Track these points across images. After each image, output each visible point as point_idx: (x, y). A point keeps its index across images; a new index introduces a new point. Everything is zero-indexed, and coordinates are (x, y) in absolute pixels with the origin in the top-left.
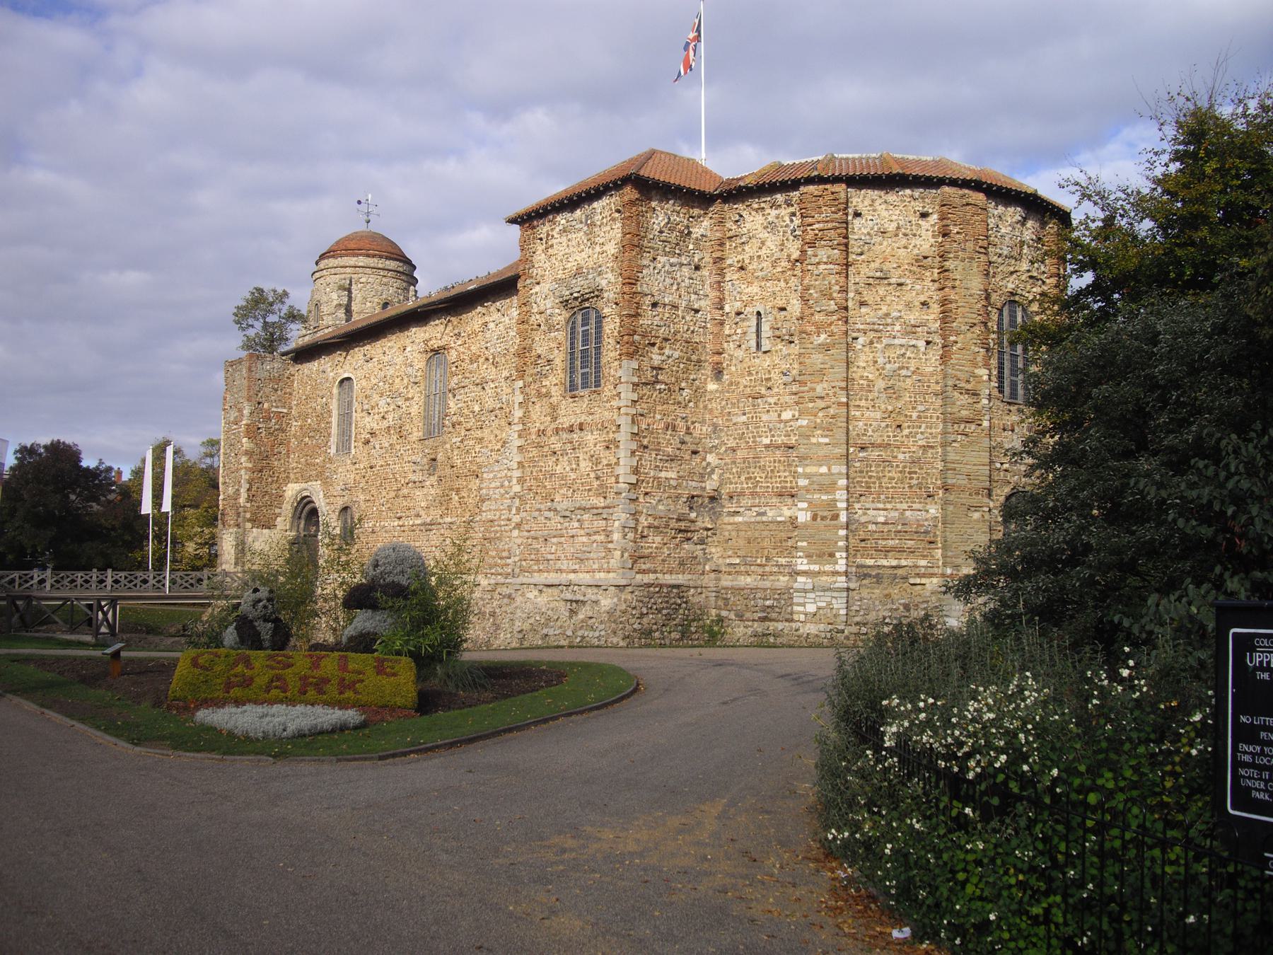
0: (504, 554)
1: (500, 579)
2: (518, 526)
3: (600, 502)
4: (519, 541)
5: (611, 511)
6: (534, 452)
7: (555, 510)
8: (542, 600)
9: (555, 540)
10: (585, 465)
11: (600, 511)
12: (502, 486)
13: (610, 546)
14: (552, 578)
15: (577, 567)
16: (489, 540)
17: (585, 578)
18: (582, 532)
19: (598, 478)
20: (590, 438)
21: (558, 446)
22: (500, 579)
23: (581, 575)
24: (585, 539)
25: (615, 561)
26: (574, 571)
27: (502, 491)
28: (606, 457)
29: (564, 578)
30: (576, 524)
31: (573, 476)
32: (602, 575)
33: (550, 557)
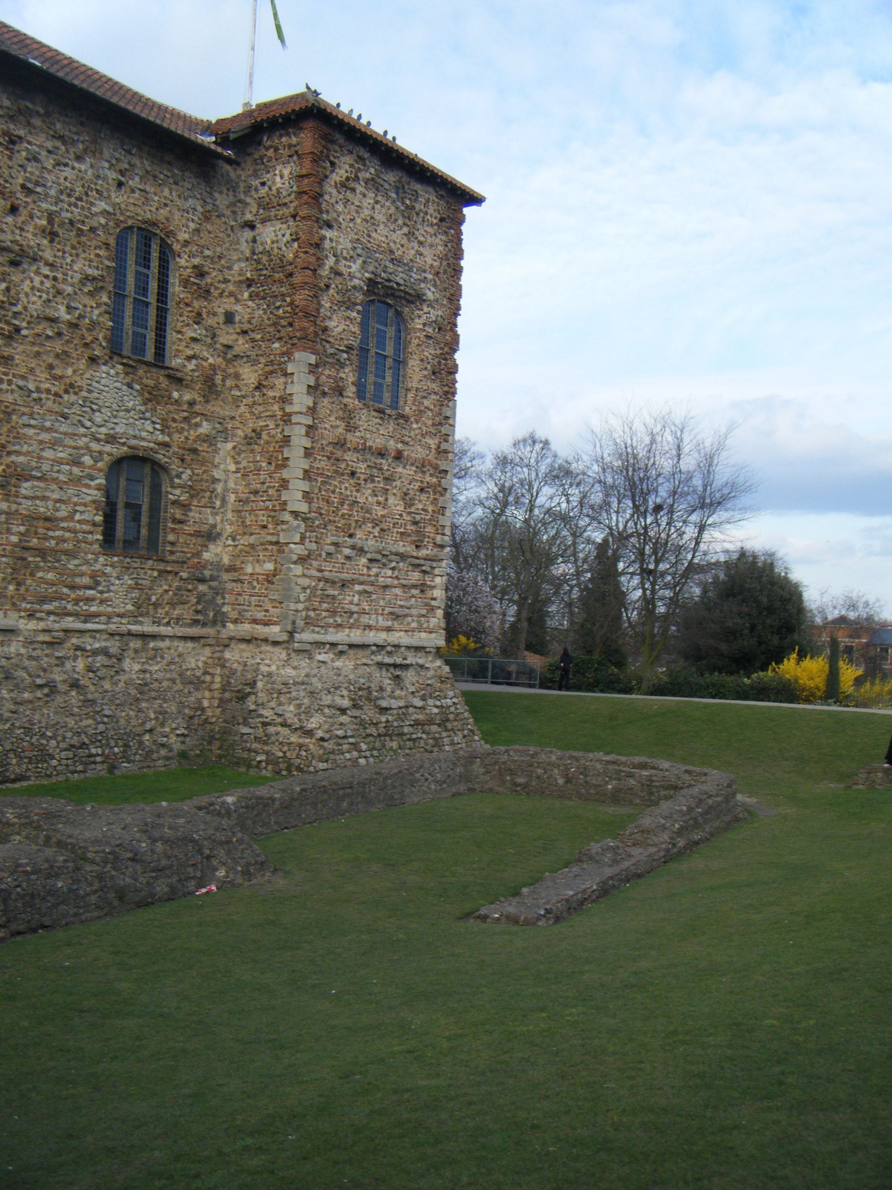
0: (86, 580)
1: (70, 623)
2: (302, 560)
3: (410, 549)
4: (305, 582)
5: (434, 564)
6: (322, 464)
7: (362, 551)
8: (346, 665)
9: (357, 587)
10: (396, 504)
11: (422, 562)
12: (76, 462)
13: (433, 603)
14: (356, 636)
15: (389, 623)
16: (42, 553)
17: (403, 639)
18: (396, 582)
19: (415, 523)
20: (405, 472)
21: (362, 468)
22: (70, 623)
23: (397, 634)
24: (398, 591)
25: (437, 619)
26: (389, 629)
27: (76, 470)
28: (423, 502)
29: (381, 637)
30: (389, 573)
31: (381, 512)
32: (423, 635)
33: (355, 609)
